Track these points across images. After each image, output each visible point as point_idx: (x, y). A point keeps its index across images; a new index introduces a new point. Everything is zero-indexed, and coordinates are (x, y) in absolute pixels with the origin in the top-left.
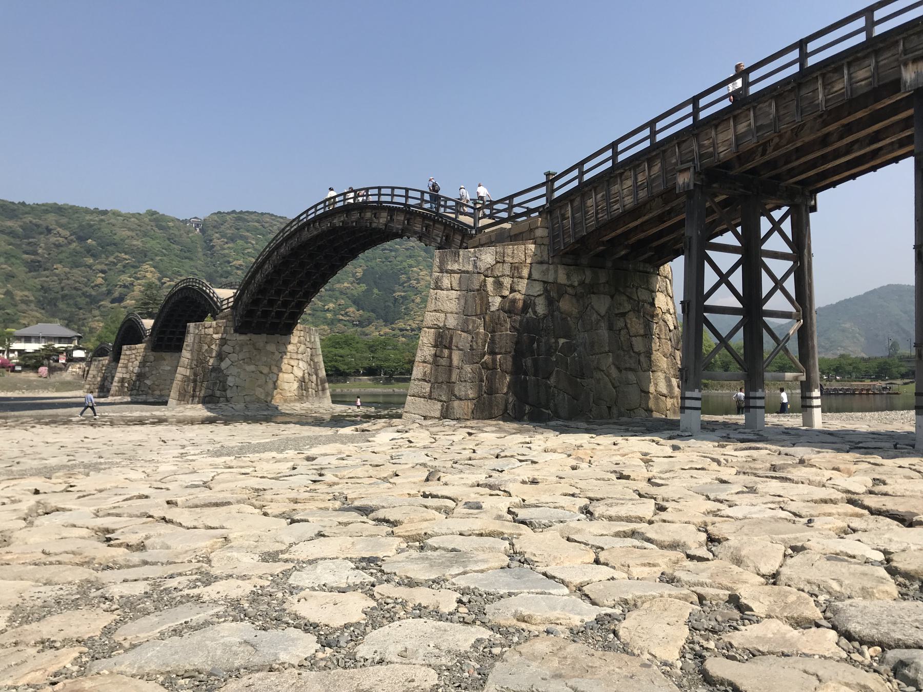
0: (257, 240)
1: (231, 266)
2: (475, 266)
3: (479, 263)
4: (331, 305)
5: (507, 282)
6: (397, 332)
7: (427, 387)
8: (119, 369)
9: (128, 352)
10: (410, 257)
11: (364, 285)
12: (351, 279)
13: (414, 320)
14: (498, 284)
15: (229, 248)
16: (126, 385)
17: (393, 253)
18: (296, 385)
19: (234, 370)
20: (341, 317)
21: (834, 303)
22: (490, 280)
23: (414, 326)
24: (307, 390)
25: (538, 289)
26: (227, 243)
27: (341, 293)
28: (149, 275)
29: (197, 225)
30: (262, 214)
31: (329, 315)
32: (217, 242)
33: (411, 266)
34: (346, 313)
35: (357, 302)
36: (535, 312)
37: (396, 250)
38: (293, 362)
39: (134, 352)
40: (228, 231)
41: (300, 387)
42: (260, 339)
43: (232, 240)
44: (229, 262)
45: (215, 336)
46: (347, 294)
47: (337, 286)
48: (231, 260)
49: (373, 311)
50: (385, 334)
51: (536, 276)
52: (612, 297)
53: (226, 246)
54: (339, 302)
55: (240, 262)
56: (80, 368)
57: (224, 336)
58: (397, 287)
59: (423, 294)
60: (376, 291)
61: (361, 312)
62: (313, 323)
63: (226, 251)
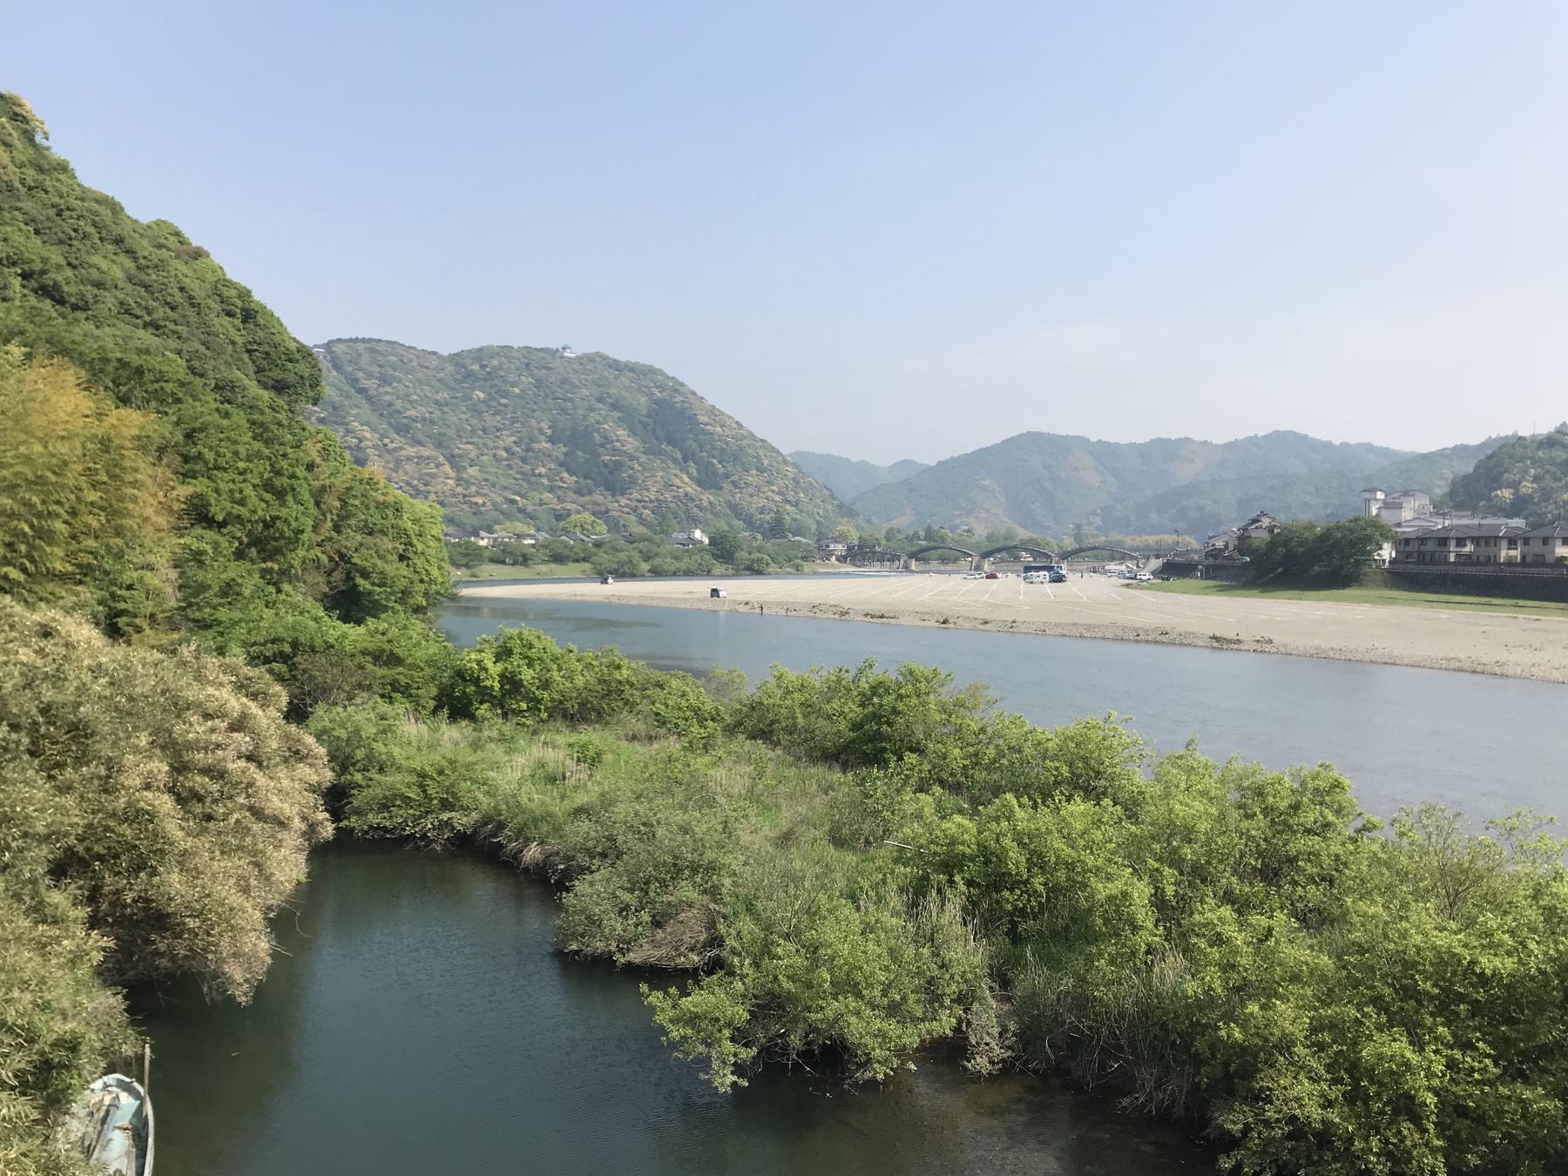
0: (410, 381)
1: (405, 417)
4: (543, 470)
6: (634, 504)
10: (592, 410)
11: (561, 445)
12: (543, 437)
13: (648, 490)
15: (387, 393)
17: (568, 404)
20: (561, 484)
21: (969, 452)
23: (653, 497)
26: (379, 385)
27: (544, 454)
28: (368, 435)
29: (325, 357)
30: (387, 342)
31: (545, 481)
32: (365, 383)
33: (598, 423)
34: (561, 479)
35: (565, 465)
37: (571, 400)
40: (373, 369)
43: (385, 382)
44: (401, 413)
46: (549, 456)
47: (535, 446)
48: (401, 409)
49: (585, 478)
50: (627, 506)
53: (381, 389)
54: (548, 466)
55: (412, 413)
58: (601, 450)
59: (642, 460)
60: (580, 453)
61: (574, 478)
62: (534, 490)
63: (387, 398)
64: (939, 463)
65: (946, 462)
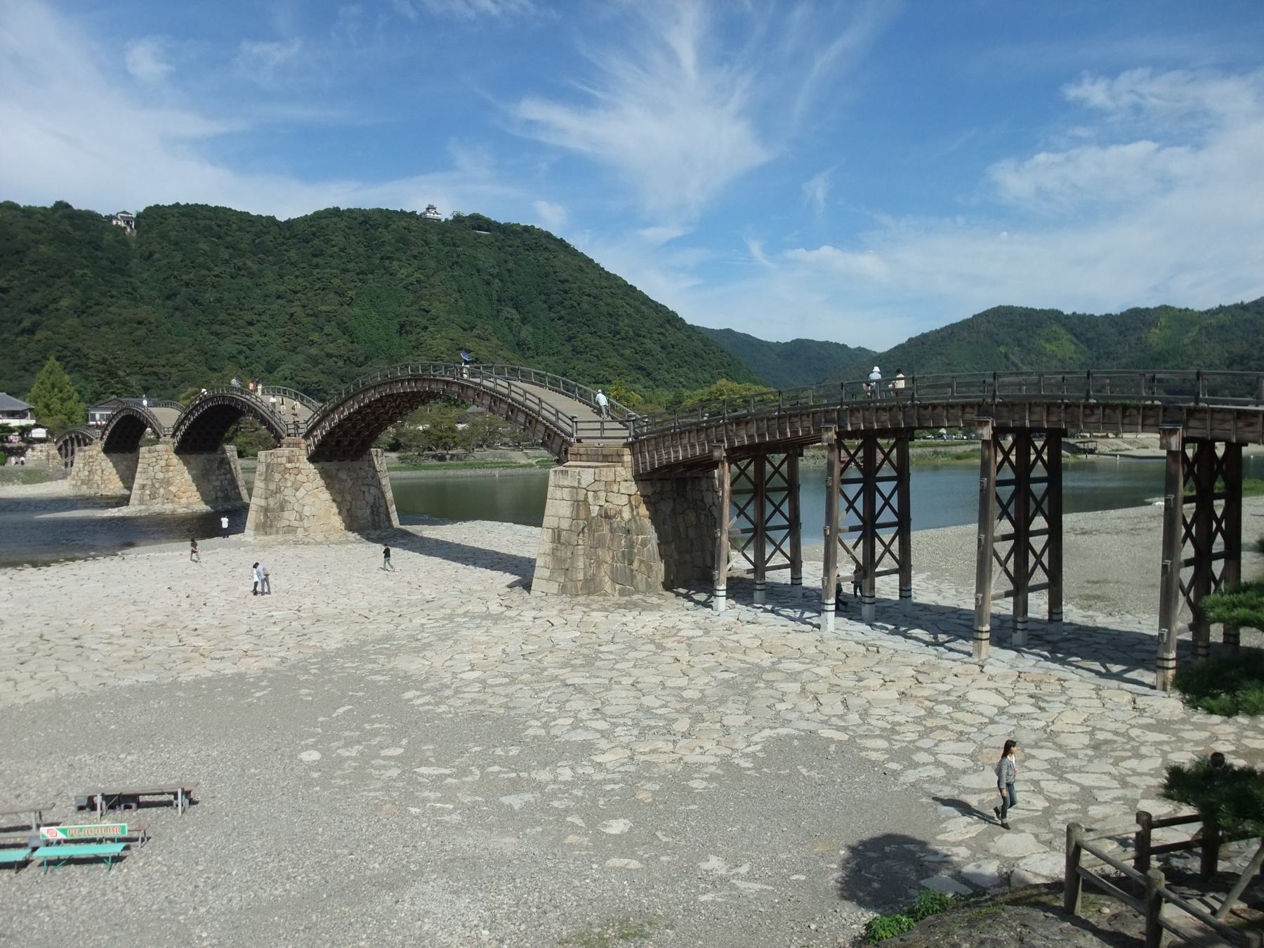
2: (579, 483)
3: (582, 481)
5: (602, 495)
7: (547, 573)
8: (138, 475)
9: (147, 455)
14: (596, 497)
16: (148, 492)
18: (368, 511)
19: (309, 500)
22: (590, 494)
24: (378, 515)
25: (625, 500)
36: (622, 517)
38: (364, 488)
39: (155, 454)
41: (372, 512)
42: (332, 466)
45: (289, 465)
51: (623, 491)
52: (674, 500)
56: (41, 451)
57: (297, 465)
64: (910, 340)
65: (917, 338)
